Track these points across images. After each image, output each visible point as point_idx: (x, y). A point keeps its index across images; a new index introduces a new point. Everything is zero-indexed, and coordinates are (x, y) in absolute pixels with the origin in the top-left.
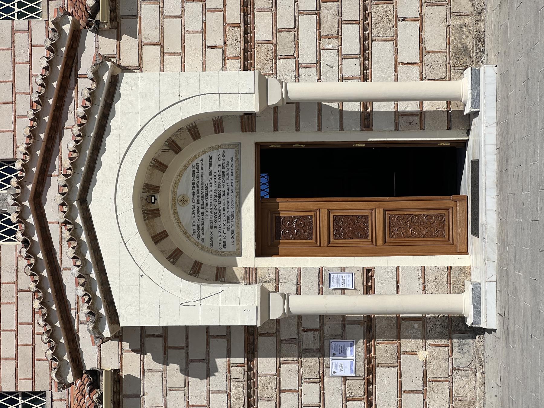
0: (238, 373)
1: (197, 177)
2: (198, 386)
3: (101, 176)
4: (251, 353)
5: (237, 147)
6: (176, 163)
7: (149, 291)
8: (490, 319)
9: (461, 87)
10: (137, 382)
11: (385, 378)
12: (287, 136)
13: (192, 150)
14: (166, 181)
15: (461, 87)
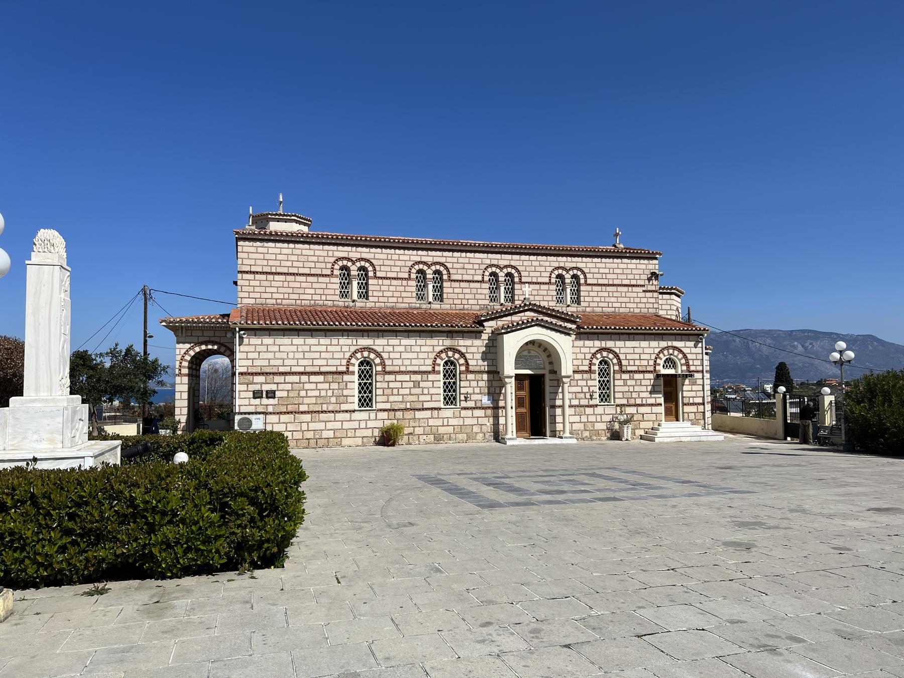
0: (483, 368)
1: (536, 357)
2: (479, 356)
3: (544, 329)
4: (488, 372)
5: (544, 369)
6: (540, 351)
7: (512, 343)
8: (509, 443)
9: (567, 434)
10: (480, 338)
11: (481, 413)
12: (547, 383)
13: (544, 355)
14: (535, 348)
15: (567, 434)
